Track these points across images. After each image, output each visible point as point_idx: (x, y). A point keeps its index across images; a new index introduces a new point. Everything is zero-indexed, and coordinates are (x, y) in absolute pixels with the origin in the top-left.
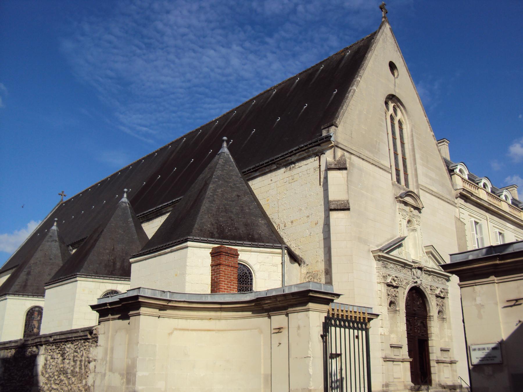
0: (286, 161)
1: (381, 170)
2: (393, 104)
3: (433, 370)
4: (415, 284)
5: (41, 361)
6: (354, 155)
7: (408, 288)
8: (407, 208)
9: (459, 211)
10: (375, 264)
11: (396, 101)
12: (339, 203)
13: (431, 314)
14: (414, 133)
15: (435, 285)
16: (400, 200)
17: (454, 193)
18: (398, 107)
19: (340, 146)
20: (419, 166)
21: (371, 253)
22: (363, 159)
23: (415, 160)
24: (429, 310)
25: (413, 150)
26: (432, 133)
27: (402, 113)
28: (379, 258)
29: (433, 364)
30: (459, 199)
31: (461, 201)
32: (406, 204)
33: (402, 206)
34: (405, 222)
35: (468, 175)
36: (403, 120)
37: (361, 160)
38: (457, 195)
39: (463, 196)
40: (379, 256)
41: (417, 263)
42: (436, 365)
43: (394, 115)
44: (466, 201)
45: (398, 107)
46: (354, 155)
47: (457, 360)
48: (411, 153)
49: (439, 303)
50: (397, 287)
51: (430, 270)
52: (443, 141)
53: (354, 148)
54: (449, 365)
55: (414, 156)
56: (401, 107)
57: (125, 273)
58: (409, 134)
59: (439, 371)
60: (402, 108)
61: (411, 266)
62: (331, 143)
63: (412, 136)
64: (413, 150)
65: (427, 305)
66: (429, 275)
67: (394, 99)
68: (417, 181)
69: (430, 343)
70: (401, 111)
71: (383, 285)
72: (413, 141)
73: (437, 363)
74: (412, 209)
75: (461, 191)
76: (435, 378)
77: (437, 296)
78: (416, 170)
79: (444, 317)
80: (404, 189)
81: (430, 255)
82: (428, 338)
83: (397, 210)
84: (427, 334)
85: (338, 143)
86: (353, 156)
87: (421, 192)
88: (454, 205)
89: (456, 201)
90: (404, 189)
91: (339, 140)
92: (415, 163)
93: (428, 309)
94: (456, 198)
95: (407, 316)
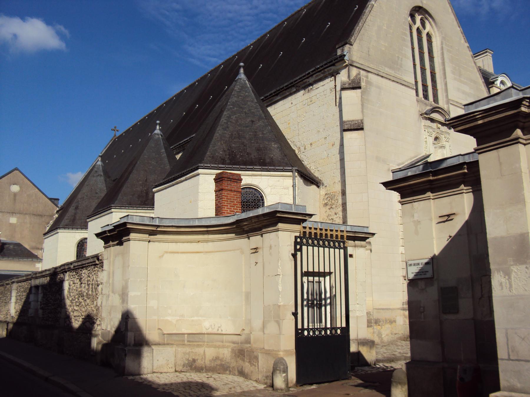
1: (403, 87)
2: (420, 17)
6: (372, 72)
8: (434, 125)
11: (423, 12)
12: (353, 123)
14: (444, 46)
16: (425, 117)
20: (448, 80)
22: (382, 77)
25: (443, 64)
26: (467, 45)
27: (431, 25)
32: (432, 120)
33: (428, 123)
34: (431, 140)
36: (432, 33)
37: (380, 78)
43: (421, 28)
45: (427, 19)
46: (372, 72)
48: (441, 67)
52: (486, 52)
53: (371, 66)
55: (444, 70)
56: (430, 18)
57: (148, 202)
62: (345, 62)
63: (442, 48)
64: (443, 64)
67: (421, 10)
68: (447, 96)
72: (443, 54)
74: (440, 126)
78: (446, 84)
80: (431, 105)
85: (353, 61)
86: (370, 74)
87: (451, 107)
90: (431, 105)
91: (354, 58)
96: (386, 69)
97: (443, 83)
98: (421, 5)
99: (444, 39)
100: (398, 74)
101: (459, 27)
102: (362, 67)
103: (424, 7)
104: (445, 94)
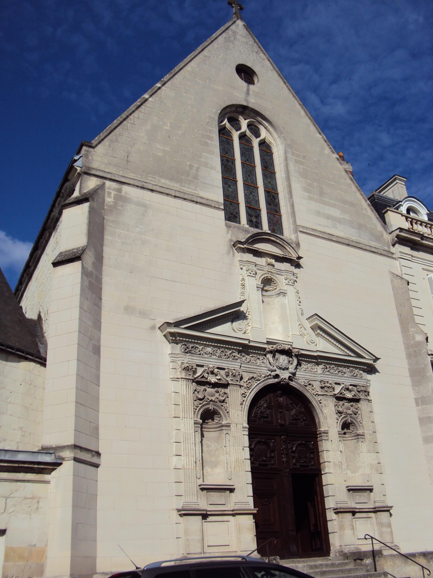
0: (53, 219)
1: (198, 206)
2: (247, 121)
3: (331, 526)
4: (276, 380)
6: (129, 184)
7: (256, 388)
8: (262, 261)
9: (400, 263)
10: (167, 348)
11: (252, 114)
12: (71, 252)
13: (322, 429)
14: (289, 155)
15: (331, 379)
16: (240, 248)
17: (389, 238)
18: (260, 123)
19: (93, 172)
20: (296, 200)
21: (159, 332)
22: (152, 191)
23: (290, 192)
24: (319, 422)
25: (288, 178)
26: (335, 156)
28: (174, 338)
29: (330, 515)
30: (397, 245)
31: (399, 249)
32: (257, 253)
33: (249, 257)
34: (256, 282)
35: (428, 215)
36: (270, 139)
37: (149, 193)
38: (393, 240)
39: (401, 241)
40: (172, 334)
41: (275, 343)
42: (334, 516)
43: (248, 133)
44: (412, 249)
45: (260, 123)
46: (129, 184)
47: (389, 505)
48: (285, 184)
49: (341, 410)
50: (226, 386)
51: (315, 354)
52: (395, 179)
53: (131, 175)
54: (372, 515)
55: (290, 186)
56: (264, 122)
58: (282, 158)
59: (342, 528)
61: (264, 349)
62: (77, 170)
63: (286, 159)
64: (288, 178)
65: (315, 415)
66: (318, 364)
67: (247, 112)
68: (295, 221)
69: (326, 479)
70: (266, 128)
71: (184, 382)
72: (287, 166)
73: (336, 513)
74: (273, 261)
75: (397, 232)
76: (335, 541)
77: (339, 398)
78: (292, 206)
79: (360, 432)
80: (246, 231)
81: (319, 331)
82: (320, 471)
83: (238, 264)
84: (319, 464)
85: (89, 168)
86: (125, 188)
87: (302, 237)
88: (389, 255)
89: (393, 249)
90: (246, 231)
91: (95, 165)
92: (291, 196)
93: (317, 421)
94: (394, 245)
95: (253, 434)
96: (163, 181)
97: (289, 205)
98: (245, 104)
100: (188, 188)
101: (320, 133)
102: (109, 176)
103: (251, 106)
104: (291, 220)
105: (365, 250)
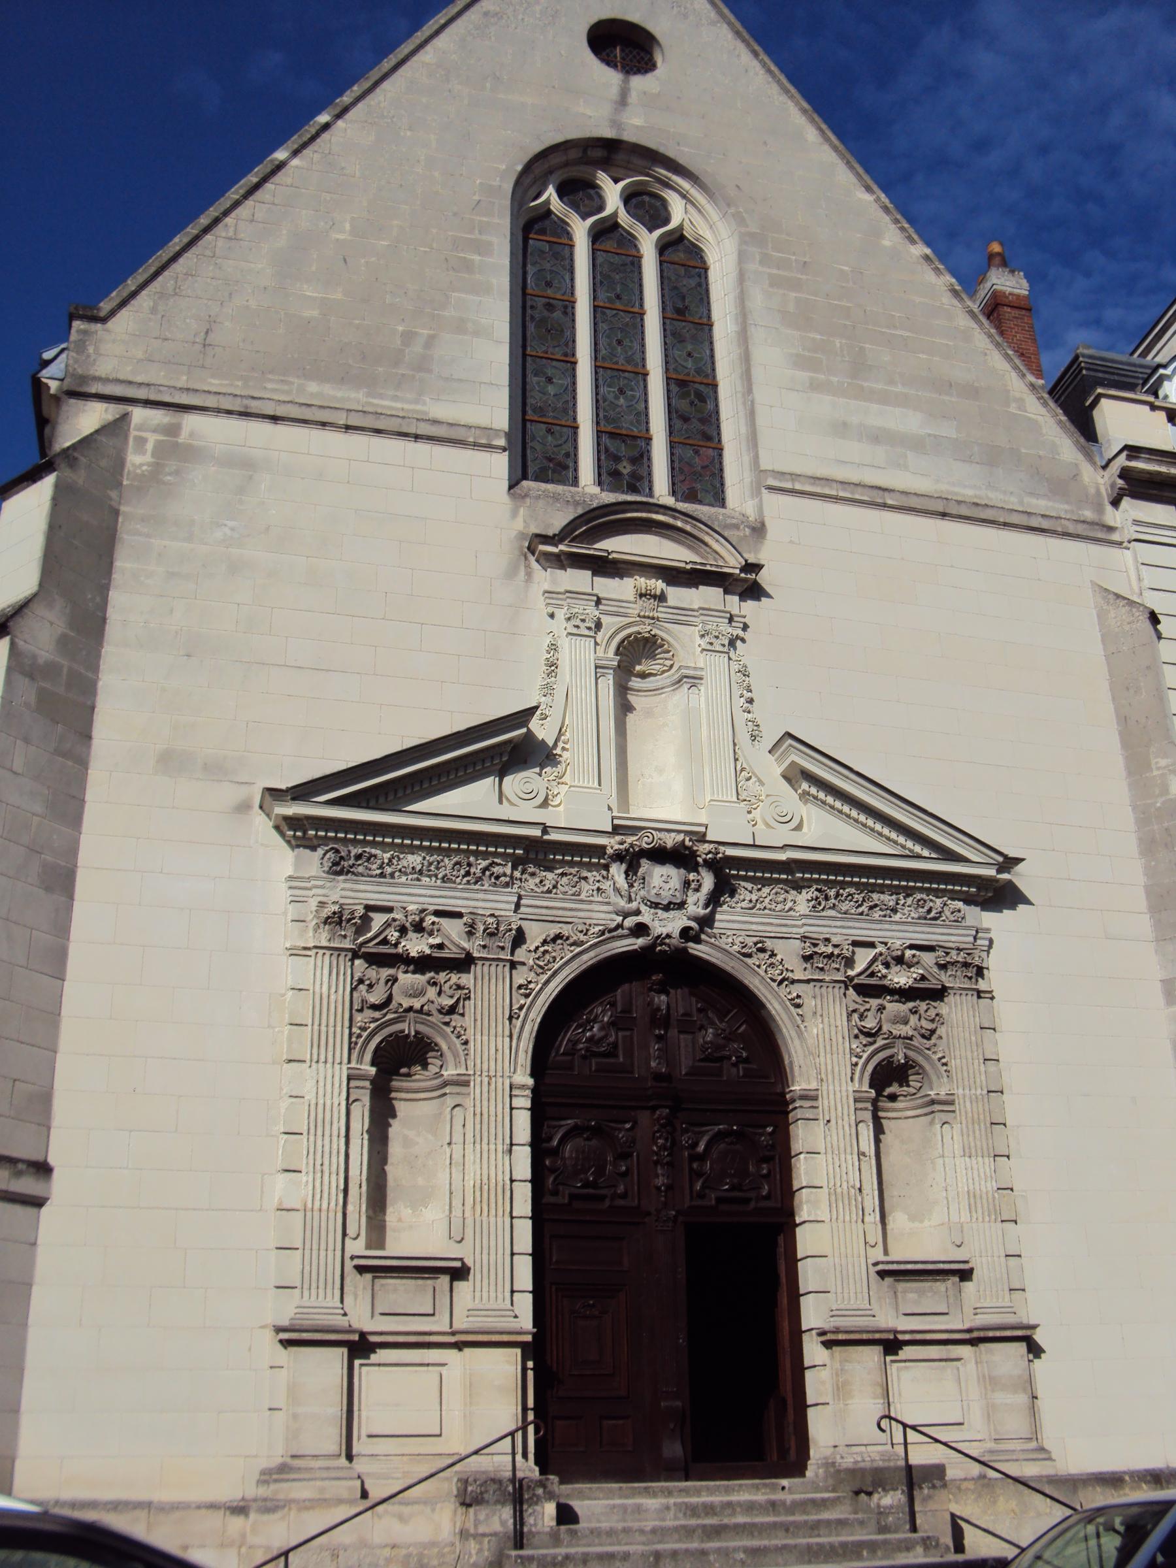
1: (423, 447)
3: (816, 1385)
4: (641, 942)
5: (537, 1473)
8: (622, 589)
10: (284, 859)
11: (638, 161)
16: (547, 555)
17: (1103, 481)
22: (275, 419)
25: (743, 336)
26: (921, 249)
28: (299, 832)
29: (813, 1351)
30: (1126, 502)
31: (1135, 512)
33: (580, 579)
37: (267, 427)
38: (1113, 485)
40: (294, 822)
41: (633, 830)
43: (624, 219)
45: (667, 185)
51: (782, 856)
53: (215, 384)
54: (965, 1351)
59: (842, 1389)
60: (685, 184)
61: (600, 850)
63: (741, 277)
65: (780, 1042)
66: (798, 886)
67: (620, 157)
68: (756, 459)
69: (806, 1240)
70: (684, 196)
73: (828, 1344)
74: (659, 585)
75: (1122, 461)
78: (752, 415)
79: (940, 1090)
81: (805, 786)
82: (792, 1214)
85: (84, 379)
86: (191, 421)
87: (775, 504)
88: (1099, 534)
89: (1112, 516)
91: (104, 368)
94: (1115, 503)
96: (313, 387)
97: (742, 414)
98: (608, 133)
99: (749, 240)
100: (395, 398)
101: (868, 189)
102: (141, 394)
103: (629, 136)
104: (746, 459)
105: (1005, 524)
